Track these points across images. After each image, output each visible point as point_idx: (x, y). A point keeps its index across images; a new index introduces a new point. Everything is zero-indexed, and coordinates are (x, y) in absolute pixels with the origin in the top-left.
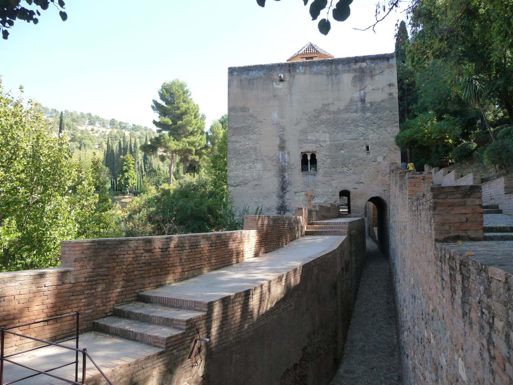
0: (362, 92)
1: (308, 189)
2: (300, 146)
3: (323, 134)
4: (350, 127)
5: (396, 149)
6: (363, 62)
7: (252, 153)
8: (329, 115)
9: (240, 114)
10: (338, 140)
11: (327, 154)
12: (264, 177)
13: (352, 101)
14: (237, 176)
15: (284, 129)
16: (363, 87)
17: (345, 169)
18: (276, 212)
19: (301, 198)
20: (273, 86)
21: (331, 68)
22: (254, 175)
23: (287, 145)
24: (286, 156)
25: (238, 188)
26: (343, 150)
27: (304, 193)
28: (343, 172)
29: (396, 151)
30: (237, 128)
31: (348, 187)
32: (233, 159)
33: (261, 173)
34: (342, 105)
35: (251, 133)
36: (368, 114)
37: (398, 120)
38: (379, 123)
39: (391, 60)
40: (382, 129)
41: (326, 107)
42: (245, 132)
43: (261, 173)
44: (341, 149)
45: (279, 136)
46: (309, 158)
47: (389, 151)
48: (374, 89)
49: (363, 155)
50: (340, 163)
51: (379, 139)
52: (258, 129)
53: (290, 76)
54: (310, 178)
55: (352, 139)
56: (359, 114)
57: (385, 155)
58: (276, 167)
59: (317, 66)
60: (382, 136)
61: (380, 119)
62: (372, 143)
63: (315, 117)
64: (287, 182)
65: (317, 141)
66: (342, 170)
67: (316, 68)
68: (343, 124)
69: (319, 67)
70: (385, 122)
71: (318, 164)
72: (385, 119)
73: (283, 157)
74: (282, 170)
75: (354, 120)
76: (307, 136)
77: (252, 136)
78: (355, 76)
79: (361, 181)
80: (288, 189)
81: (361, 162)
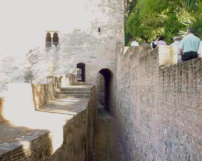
50: (77, 41)
71: (60, 41)
79: (94, 56)
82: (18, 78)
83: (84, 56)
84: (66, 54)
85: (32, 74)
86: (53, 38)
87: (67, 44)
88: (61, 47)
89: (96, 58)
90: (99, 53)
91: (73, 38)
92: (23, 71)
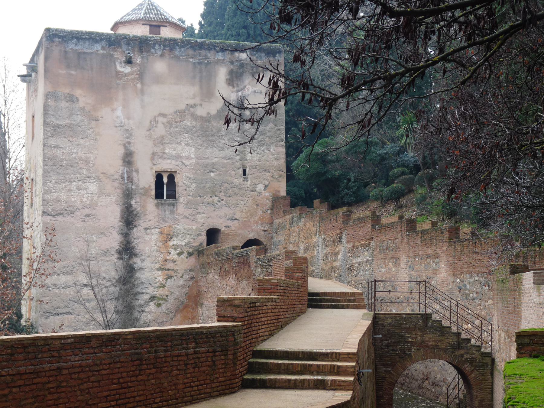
1: (164, 225)
3: (187, 148)
5: (280, 176)
6: (243, 52)
7: (81, 166)
8: (196, 121)
10: (207, 158)
11: (192, 176)
12: (99, 204)
14: (58, 200)
15: (131, 135)
16: (242, 87)
17: (216, 199)
18: (116, 256)
20: (116, 69)
22: (85, 199)
25: (59, 218)
26: (213, 172)
27: (157, 230)
28: (213, 204)
29: (280, 179)
30: (58, 126)
31: (219, 223)
33: (95, 198)
35: (81, 136)
37: (283, 137)
38: (260, 139)
39: (278, 55)
40: (264, 148)
41: (192, 110)
42: (71, 133)
43: (95, 198)
44: (211, 171)
45: (124, 145)
46: (165, 180)
47: (272, 179)
48: (255, 92)
49: (239, 181)
50: (208, 190)
51: (259, 160)
53: (142, 58)
55: (224, 158)
57: (267, 183)
58: (118, 191)
59: (180, 48)
60: (264, 158)
62: (251, 166)
63: (176, 122)
64: (135, 212)
65: (177, 157)
66: (210, 200)
67: (178, 50)
70: (267, 139)
71: (179, 190)
72: (269, 134)
74: (128, 195)
76: (164, 149)
77: (82, 141)
79: (236, 217)
80: (135, 223)
81: (236, 190)
82: (106, 251)
83: (219, 217)
86: (166, 184)
87: (191, 194)
88: (181, 200)
89: (238, 220)
90: (244, 211)
91: (202, 185)
92: (115, 240)
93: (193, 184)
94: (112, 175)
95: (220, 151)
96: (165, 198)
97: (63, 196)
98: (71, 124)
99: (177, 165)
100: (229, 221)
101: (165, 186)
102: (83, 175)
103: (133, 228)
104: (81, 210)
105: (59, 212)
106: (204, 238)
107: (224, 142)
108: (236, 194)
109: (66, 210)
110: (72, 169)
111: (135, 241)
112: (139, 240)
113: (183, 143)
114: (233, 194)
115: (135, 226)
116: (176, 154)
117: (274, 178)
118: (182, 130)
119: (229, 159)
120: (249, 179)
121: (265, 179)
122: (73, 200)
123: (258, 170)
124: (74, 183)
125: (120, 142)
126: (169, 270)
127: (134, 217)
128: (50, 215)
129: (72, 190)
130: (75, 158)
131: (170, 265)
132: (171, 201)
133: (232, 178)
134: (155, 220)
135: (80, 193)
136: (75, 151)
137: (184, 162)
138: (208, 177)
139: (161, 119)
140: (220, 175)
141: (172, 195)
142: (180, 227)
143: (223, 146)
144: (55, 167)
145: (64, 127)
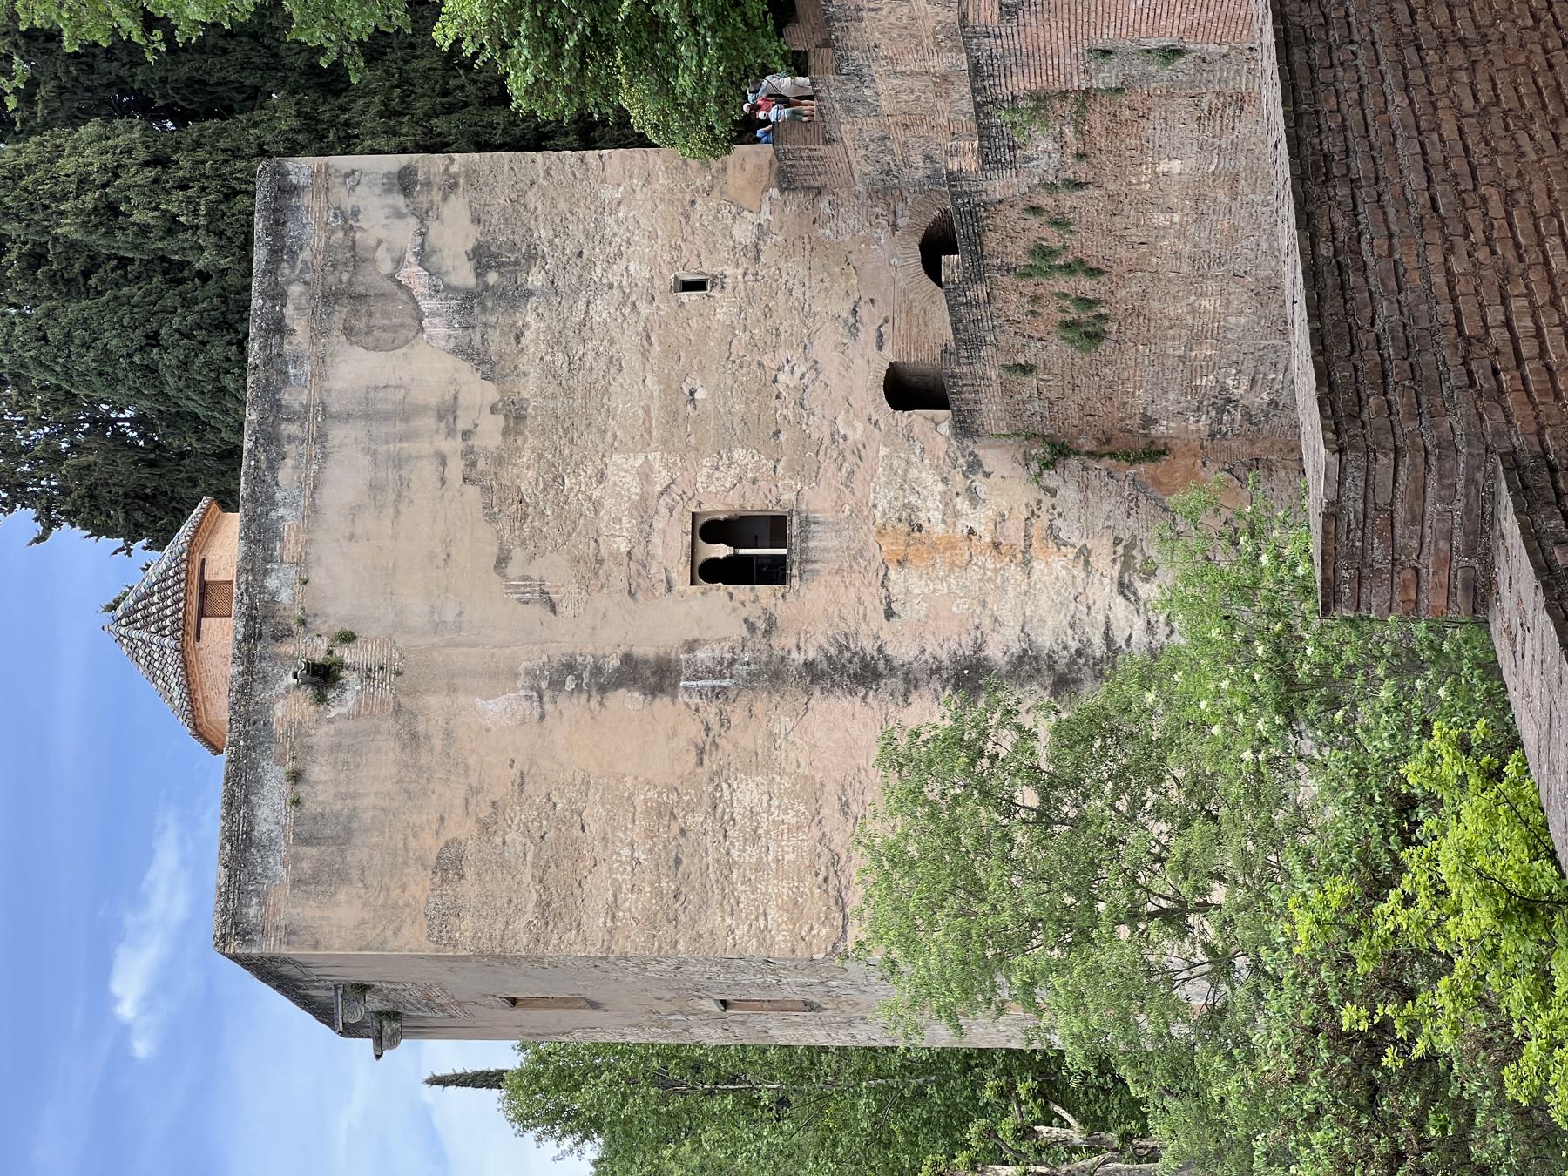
0: (425, 305)
2: (662, 588)
4: (590, 355)
7: (675, 830)
9: (469, 888)
10: (647, 412)
11: (708, 462)
12: (805, 770)
13: (464, 352)
14: (794, 905)
15: (570, 667)
19: (918, 586)
21: (290, 438)
22: (790, 818)
23: (646, 650)
24: (702, 655)
25: (854, 899)
27: (892, 575)
30: (544, 906)
32: (703, 928)
33: (786, 782)
34: (478, 392)
36: (535, 279)
39: (294, 179)
40: (610, 221)
42: (567, 864)
43: (786, 782)
45: (603, 689)
46: (722, 551)
49: (721, 305)
51: (653, 236)
52: (555, 797)
54: (821, 541)
55: (645, 353)
56: (530, 318)
58: (759, 707)
59: (274, 505)
61: (560, 229)
62: (672, 266)
63: (526, 515)
64: (833, 651)
65: (643, 512)
67: (281, 511)
68: (568, 392)
69: (279, 496)
71: (755, 502)
72: (562, 206)
73: (711, 673)
74: (773, 674)
75: (557, 342)
76: (615, 556)
77: (593, 827)
78: (348, 331)
79: (844, 315)
80: (871, 649)
81: (753, 312)
83: (848, 368)
84: (833, 468)
85: (947, 663)
87: (771, 464)
88: (788, 497)
91: (738, 426)
93: (735, 456)
94: (708, 730)
95: (620, 370)
96: (784, 551)
97: (777, 889)
98: (535, 865)
99: (671, 512)
100: (862, 335)
101: (742, 551)
102: (708, 826)
103: (887, 660)
104: (827, 830)
105: (832, 901)
106: (918, 418)
107: (590, 355)
108: (768, 312)
109: (826, 880)
110: (685, 861)
111: (929, 649)
112: (928, 635)
113: (596, 494)
114: (769, 323)
115: (880, 650)
116: (631, 516)
117: (712, 187)
118: (550, 497)
119: (649, 337)
120: (717, 270)
121: (715, 218)
122: (791, 857)
123: (684, 240)
124: (735, 853)
125: (594, 703)
126: (1027, 536)
127: (847, 655)
128: (845, 931)
129: (760, 861)
130: (651, 851)
131: (1013, 533)
132: (794, 530)
133: (715, 325)
134: (857, 583)
135: (767, 832)
136: (626, 851)
137: (659, 488)
138: (710, 407)
139: (514, 569)
140: (702, 369)
141: (776, 527)
142: (884, 499)
143: (604, 359)
144: (681, 918)
145: (546, 888)
